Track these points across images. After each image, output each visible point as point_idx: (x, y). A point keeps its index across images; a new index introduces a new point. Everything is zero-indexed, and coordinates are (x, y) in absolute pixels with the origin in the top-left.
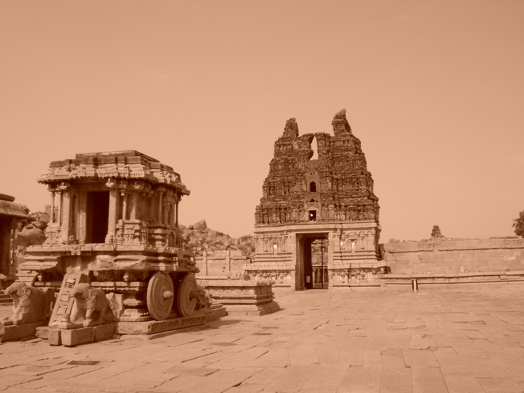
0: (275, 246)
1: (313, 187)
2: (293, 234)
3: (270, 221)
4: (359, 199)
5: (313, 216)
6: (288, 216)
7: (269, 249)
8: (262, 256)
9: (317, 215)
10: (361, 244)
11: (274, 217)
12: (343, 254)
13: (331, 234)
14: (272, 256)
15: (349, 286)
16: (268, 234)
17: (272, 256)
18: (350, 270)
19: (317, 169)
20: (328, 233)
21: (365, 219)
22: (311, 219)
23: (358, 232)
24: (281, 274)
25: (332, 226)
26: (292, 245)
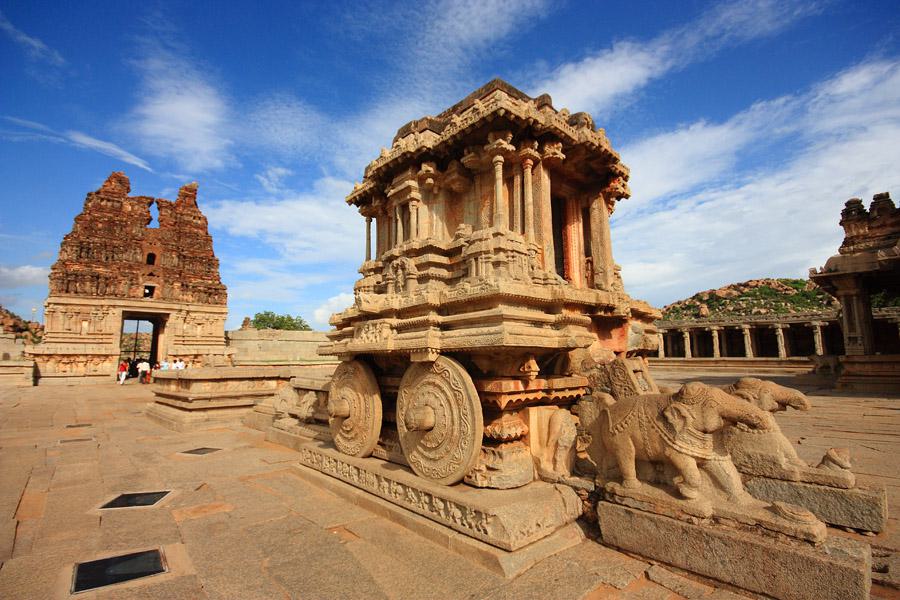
0: (85, 324)
1: (151, 259)
2: (118, 312)
4: (210, 282)
7: (73, 327)
8: (60, 335)
10: (208, 328)
11: (88, 286)
13: (173, 315)
14: (78, 336)
17: (78, 336)
18: (196, 356)
19: (160, 240)
20: (168, 314)
22: (146, 295)
24: (96, 360)
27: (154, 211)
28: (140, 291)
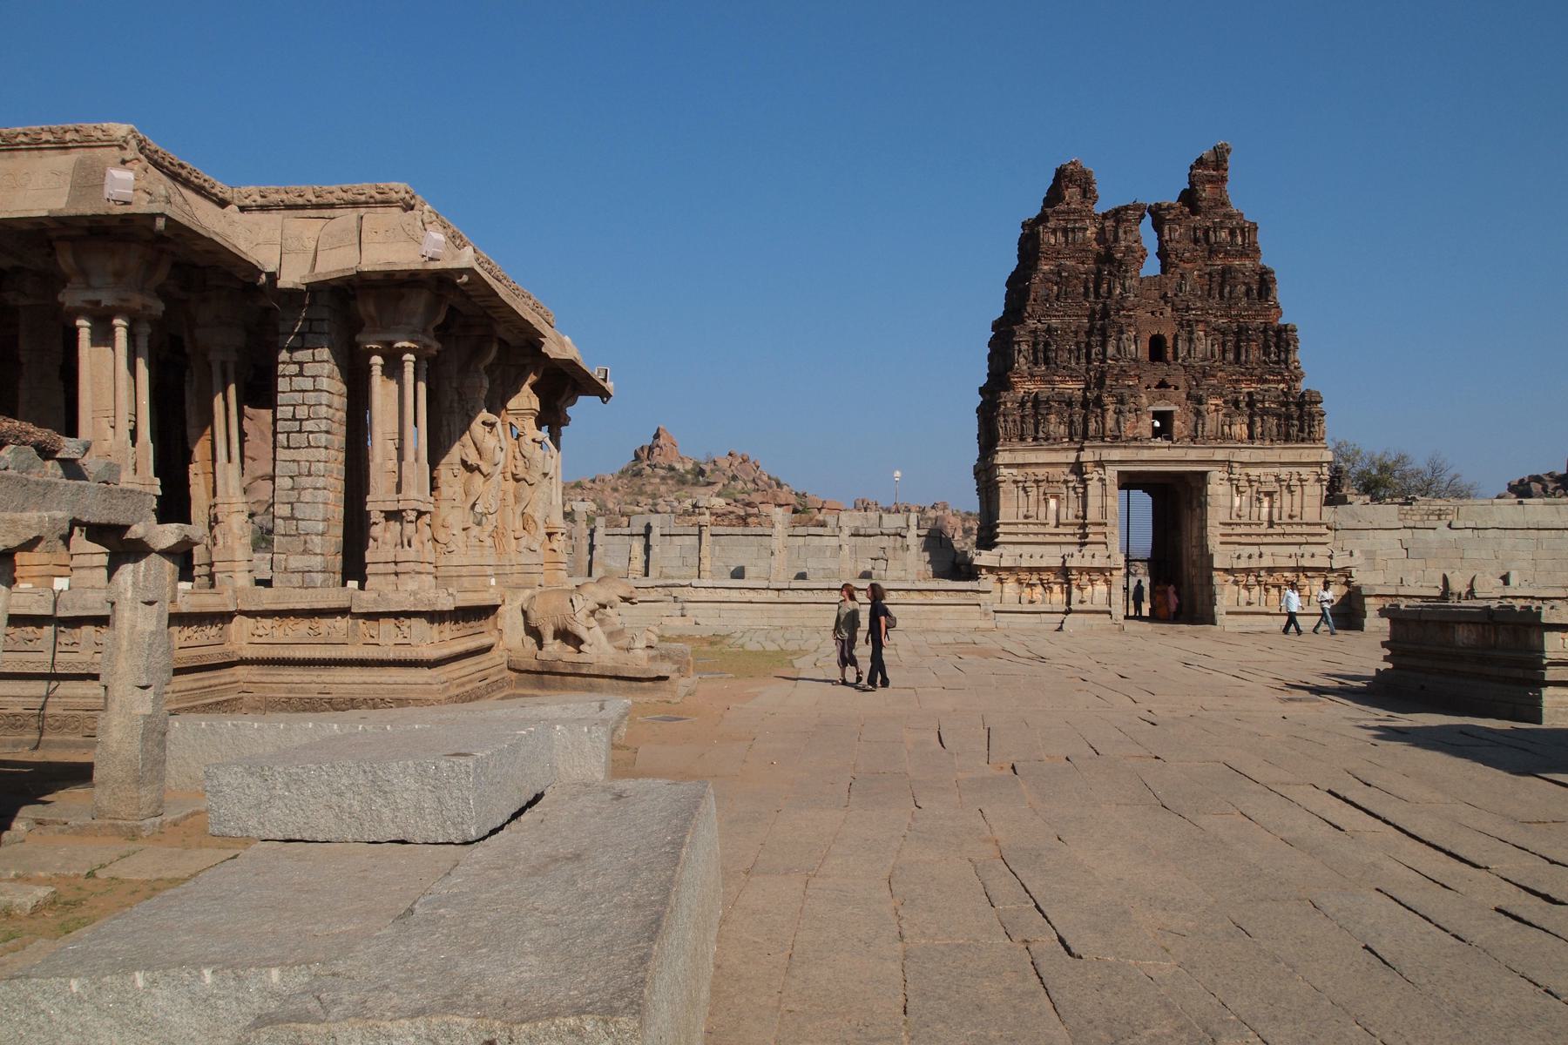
1: (1157, 348)
2: (1111, 473)
3: (1041, 435)
5: (1164, 426)
6: (1092, 426)
8: (1021, 528)
9: (1176, 423)
12: (1238, 530)
13: (1216, 475)
15: (1267, 614)
16: (1036, 470)
21: (1303, 440)
22: (1156, 433)
23: (1284, 472)
25: (1220, 455)
26: (1106, 499)
27: (1147, 234)
28: (1147, 424)
